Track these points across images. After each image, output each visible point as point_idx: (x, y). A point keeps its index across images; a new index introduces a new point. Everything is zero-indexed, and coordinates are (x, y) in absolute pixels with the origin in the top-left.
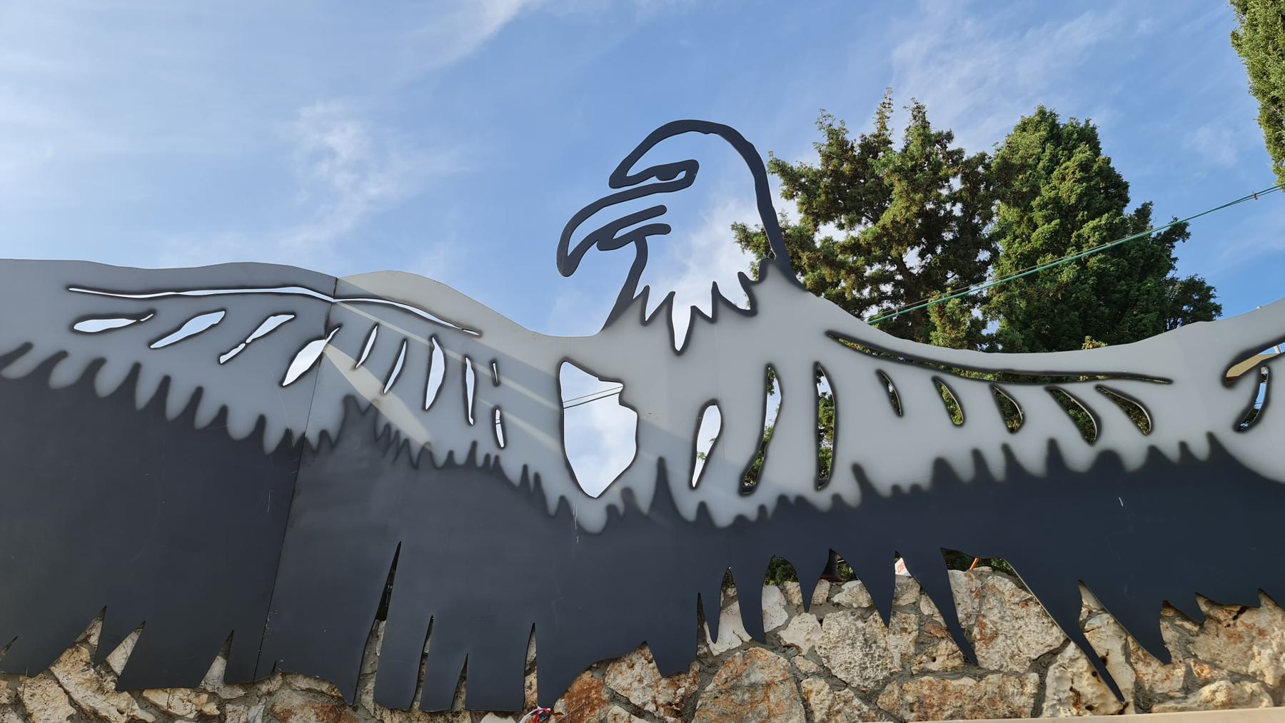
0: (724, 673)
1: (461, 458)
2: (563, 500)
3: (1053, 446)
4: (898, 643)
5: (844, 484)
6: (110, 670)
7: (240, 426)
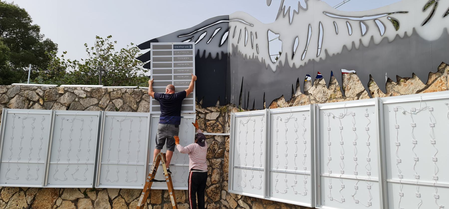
0: (297, 100)
1: (251, 57)
2: (269, 65)
3: (372, 38)
4: (330, 92)
5: (323, 55)
7: (214, 56)
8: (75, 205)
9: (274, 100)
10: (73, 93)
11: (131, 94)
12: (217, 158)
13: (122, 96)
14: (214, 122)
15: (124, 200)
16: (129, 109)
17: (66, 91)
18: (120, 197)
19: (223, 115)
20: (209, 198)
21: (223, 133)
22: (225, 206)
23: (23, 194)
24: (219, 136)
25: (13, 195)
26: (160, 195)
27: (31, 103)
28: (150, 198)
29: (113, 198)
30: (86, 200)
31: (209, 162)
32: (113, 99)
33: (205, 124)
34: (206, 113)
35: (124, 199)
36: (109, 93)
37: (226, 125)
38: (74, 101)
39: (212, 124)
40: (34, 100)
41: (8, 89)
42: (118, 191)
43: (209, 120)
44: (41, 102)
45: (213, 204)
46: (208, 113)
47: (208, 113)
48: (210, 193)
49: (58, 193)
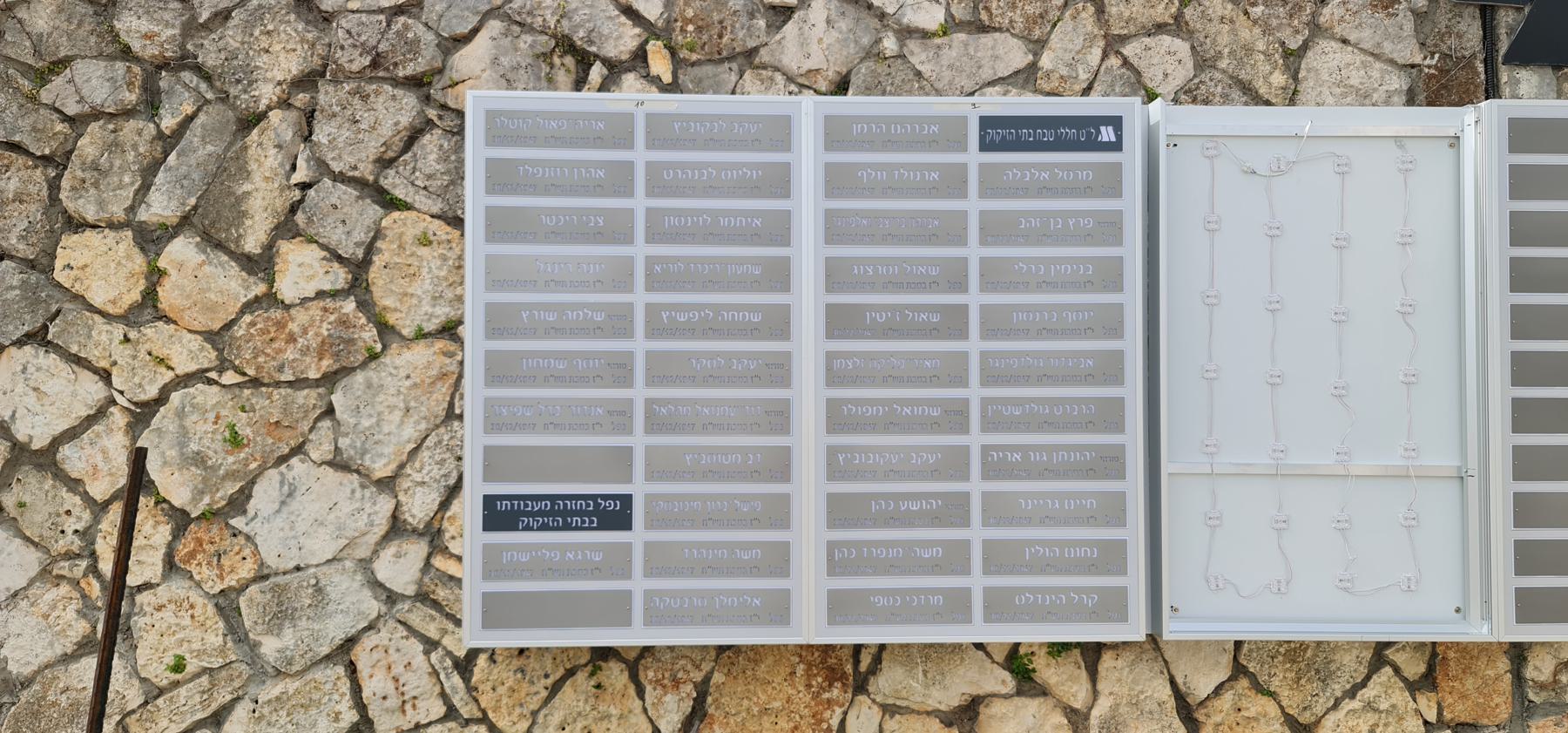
15: (1272, 709)
18: (1244, 683)
23: (624, 678)
25: (555, 689)
26: (1503, 664)
28: (1434, 687)
32: (1123, 39)
38: (873, 53)
40: (611, 51)
44: (660, 64)
49: (849, 668)
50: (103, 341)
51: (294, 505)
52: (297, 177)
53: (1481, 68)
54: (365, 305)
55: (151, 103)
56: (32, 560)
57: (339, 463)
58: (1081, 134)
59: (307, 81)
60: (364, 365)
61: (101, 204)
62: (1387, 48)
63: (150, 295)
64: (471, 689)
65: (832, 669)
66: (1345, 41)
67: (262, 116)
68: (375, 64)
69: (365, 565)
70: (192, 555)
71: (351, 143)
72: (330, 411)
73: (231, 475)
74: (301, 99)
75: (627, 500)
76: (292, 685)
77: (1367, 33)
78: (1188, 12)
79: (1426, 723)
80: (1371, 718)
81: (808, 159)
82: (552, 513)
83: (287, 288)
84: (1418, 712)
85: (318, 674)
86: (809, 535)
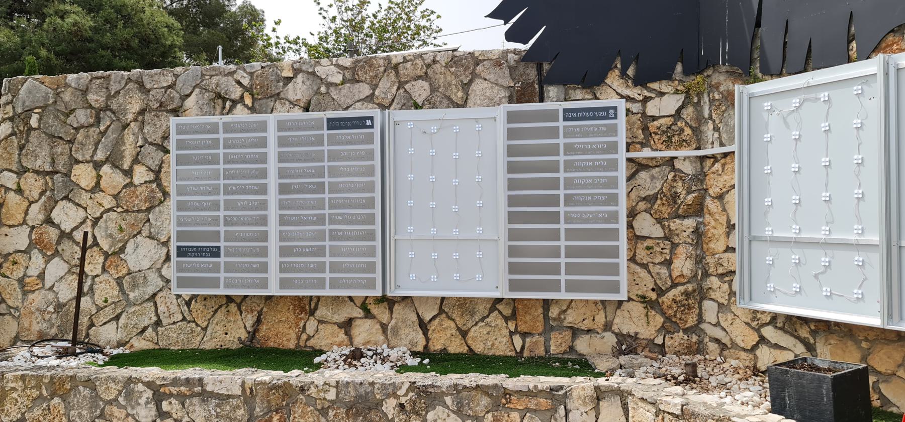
6: (629, 78)
8: (346, 334)
9: (892, 31)
10: (313, 74)
11: (447, 66)
12: (683, 217)
13: (426, 73)
14: (669, 121)
15: (453, 325)
16: (445, 102)
17: (297, 71)
18: (444, 315)
19: (696, 100)
20: (668, 319)
21: (698, 148)
22: (717, 341)
24: (685, 158)
25: (216, 312)
26: (540, 311)
27: (228, 105)
28: (515, 319)
29: (427, 317)
30: (368, 322)
31: (663, 227)
32: (407, 82)
33: (645, 129)
34: (646, 100)
35: (453, 320)
36: (396, 67)
37: (704, 128)
38: (318, 92)
39: (664, 128)
40: (233, 97)
41: (177, 76)
42: (439, 302)
43: (654, 118)
44: (248, 101)
45: (681, 333)
46: (651, 98)
47: (651, 98)
48: (670, 307)
49: (307, 307)
50: (84, 198)
51: (138, 250)
52: (139, 144)
53: (537, 86)
54: (159, 185)
55: (98, 121)
56: (66, 267)
57: (151, 237)
58: (360, 123)
59: (142, 112)
60: (159, 205)
61: (83, 155)
62: (500, 81)
63: (98, 184)
64: (190, 311)
65: (302, 308)
66: (485, 79)
67: (128, 125)
68: (160, 106)
69: (159, 270)
70: (110, 266)
71: (154, 132)
72: (149, 220)
73: (120, 241)
74: (140, 118)
75: (219, 248)
76: (138, 308)
77: (492, 76)
78: (429, 71)
79: (511, 332)
80: (488, 329)
81: (272, 135)
82: (197, 252)
83: (136, 181)
84: (507, 327)
85: (145, 305)
86: (273, 260)
